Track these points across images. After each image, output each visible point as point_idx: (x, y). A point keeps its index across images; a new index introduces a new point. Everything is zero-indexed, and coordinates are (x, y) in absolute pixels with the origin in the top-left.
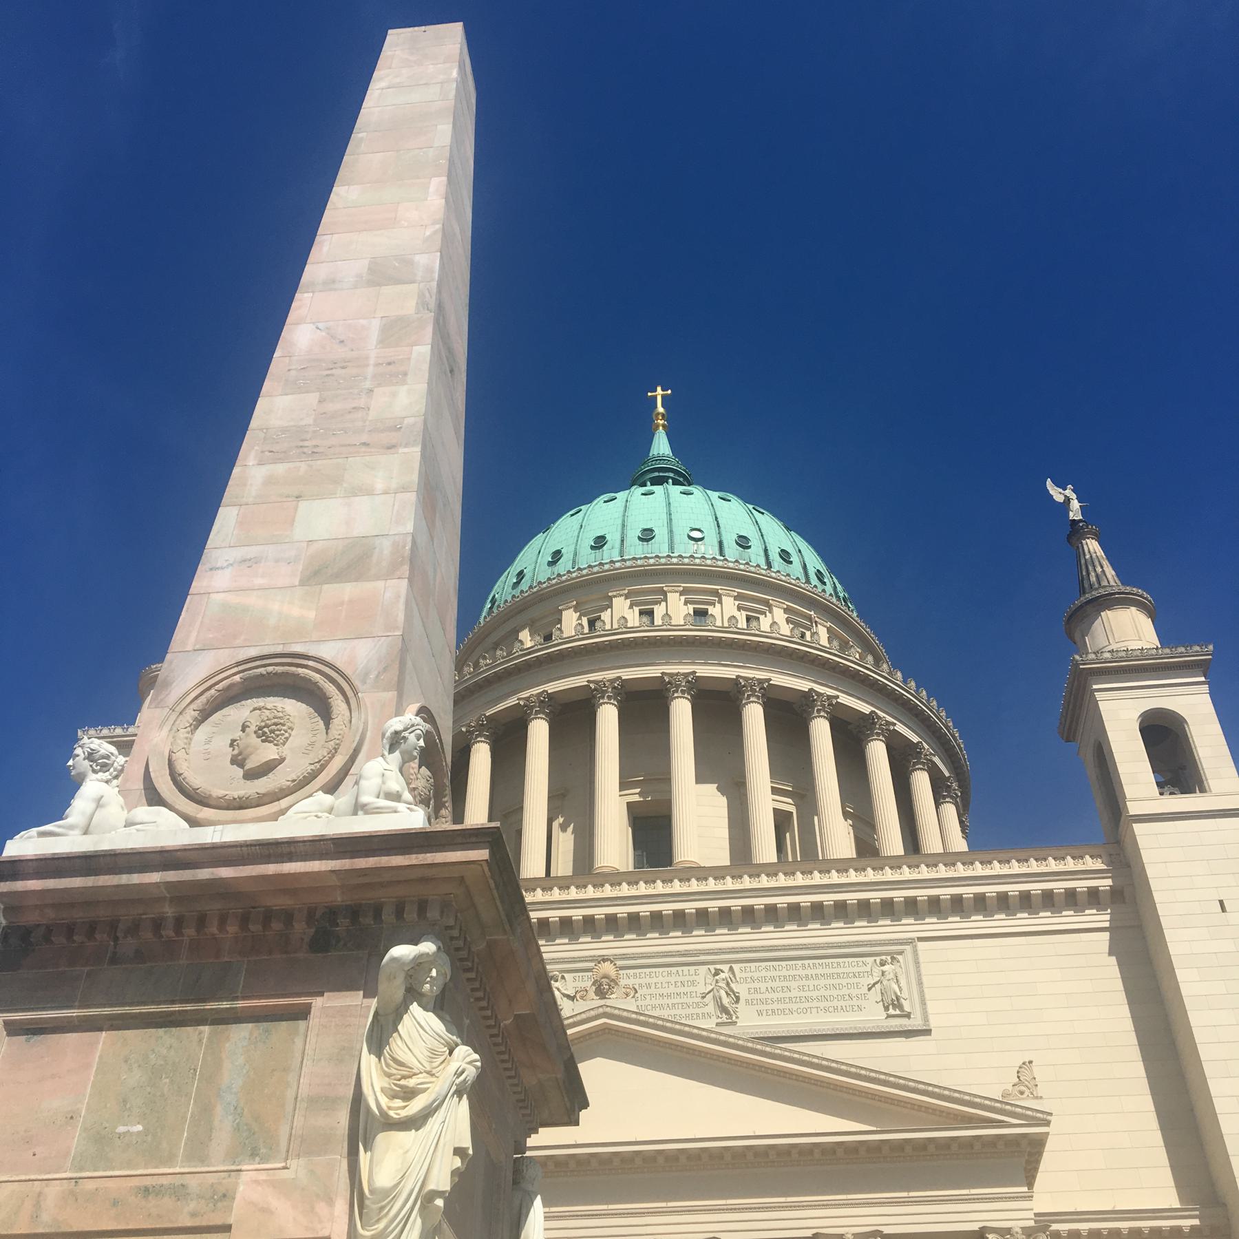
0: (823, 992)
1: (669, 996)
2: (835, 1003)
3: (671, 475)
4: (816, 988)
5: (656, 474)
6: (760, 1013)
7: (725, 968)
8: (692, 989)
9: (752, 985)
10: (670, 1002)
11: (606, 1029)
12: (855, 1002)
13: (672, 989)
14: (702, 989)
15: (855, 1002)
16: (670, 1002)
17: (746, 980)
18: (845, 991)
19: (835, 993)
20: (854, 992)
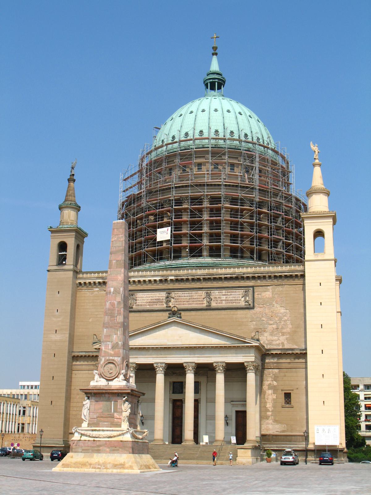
0: (231, 299)
1: (196, 299)
2: (234, 301)
3: (217, 80)
4: (230, 297)
5: (211, 80)
6: (216, 303)
7: (209, 292)
8: (201, 297)
9: (215, 296)
10: (196, 300)
11: (174, 321)
12: (238, 301)
13: (196, 297)
14: (203, 297)
15: (238, 301)
16: (196, 300)
17: (215, 294)
18: (236, 298)
19: (234, 299)
20: (238, 299)
